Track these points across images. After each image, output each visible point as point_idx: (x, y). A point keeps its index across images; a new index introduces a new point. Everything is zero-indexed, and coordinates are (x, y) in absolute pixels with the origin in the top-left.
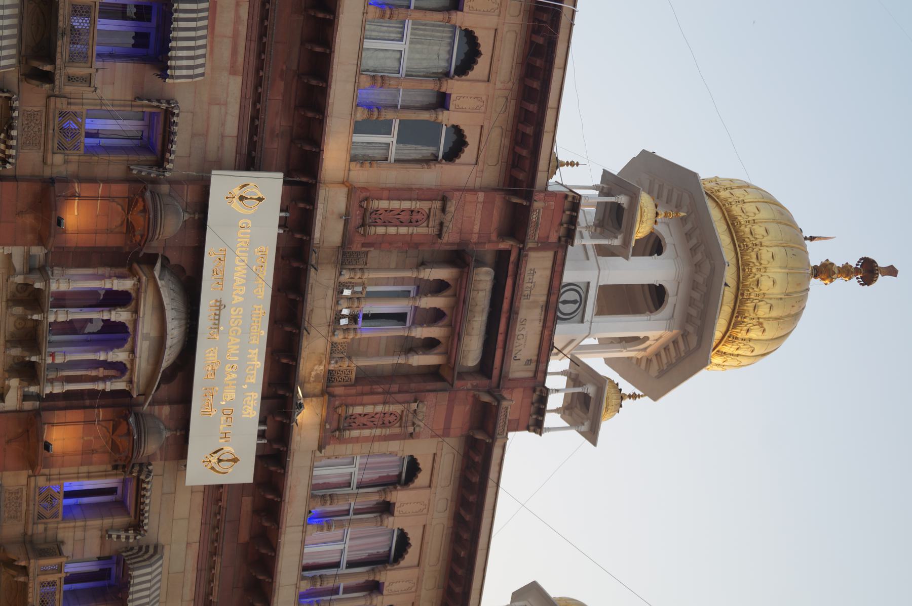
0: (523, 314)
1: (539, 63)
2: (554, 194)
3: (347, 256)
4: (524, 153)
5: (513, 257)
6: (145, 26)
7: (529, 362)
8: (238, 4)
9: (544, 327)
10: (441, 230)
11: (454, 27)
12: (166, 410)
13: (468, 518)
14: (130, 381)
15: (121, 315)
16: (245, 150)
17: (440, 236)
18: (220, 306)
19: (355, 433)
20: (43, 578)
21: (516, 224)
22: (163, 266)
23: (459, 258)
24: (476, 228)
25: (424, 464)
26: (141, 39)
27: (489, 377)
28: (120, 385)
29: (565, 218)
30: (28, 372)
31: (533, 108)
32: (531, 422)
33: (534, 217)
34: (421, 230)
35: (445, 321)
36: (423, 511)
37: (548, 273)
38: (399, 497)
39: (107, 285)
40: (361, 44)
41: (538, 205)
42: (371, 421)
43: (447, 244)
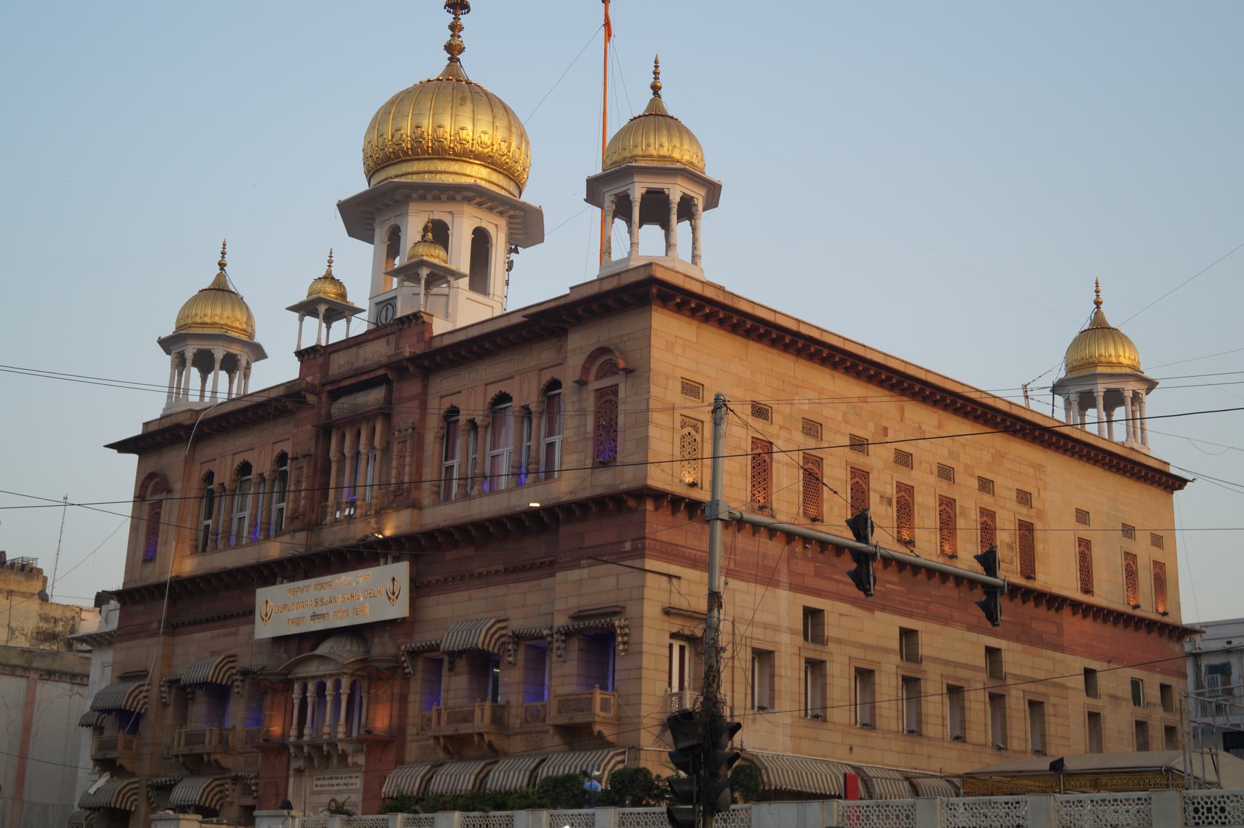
5: (329, 388)
9: (368, 341)
15: (311, 687)
18: (315, 616)
43: (316, 446)
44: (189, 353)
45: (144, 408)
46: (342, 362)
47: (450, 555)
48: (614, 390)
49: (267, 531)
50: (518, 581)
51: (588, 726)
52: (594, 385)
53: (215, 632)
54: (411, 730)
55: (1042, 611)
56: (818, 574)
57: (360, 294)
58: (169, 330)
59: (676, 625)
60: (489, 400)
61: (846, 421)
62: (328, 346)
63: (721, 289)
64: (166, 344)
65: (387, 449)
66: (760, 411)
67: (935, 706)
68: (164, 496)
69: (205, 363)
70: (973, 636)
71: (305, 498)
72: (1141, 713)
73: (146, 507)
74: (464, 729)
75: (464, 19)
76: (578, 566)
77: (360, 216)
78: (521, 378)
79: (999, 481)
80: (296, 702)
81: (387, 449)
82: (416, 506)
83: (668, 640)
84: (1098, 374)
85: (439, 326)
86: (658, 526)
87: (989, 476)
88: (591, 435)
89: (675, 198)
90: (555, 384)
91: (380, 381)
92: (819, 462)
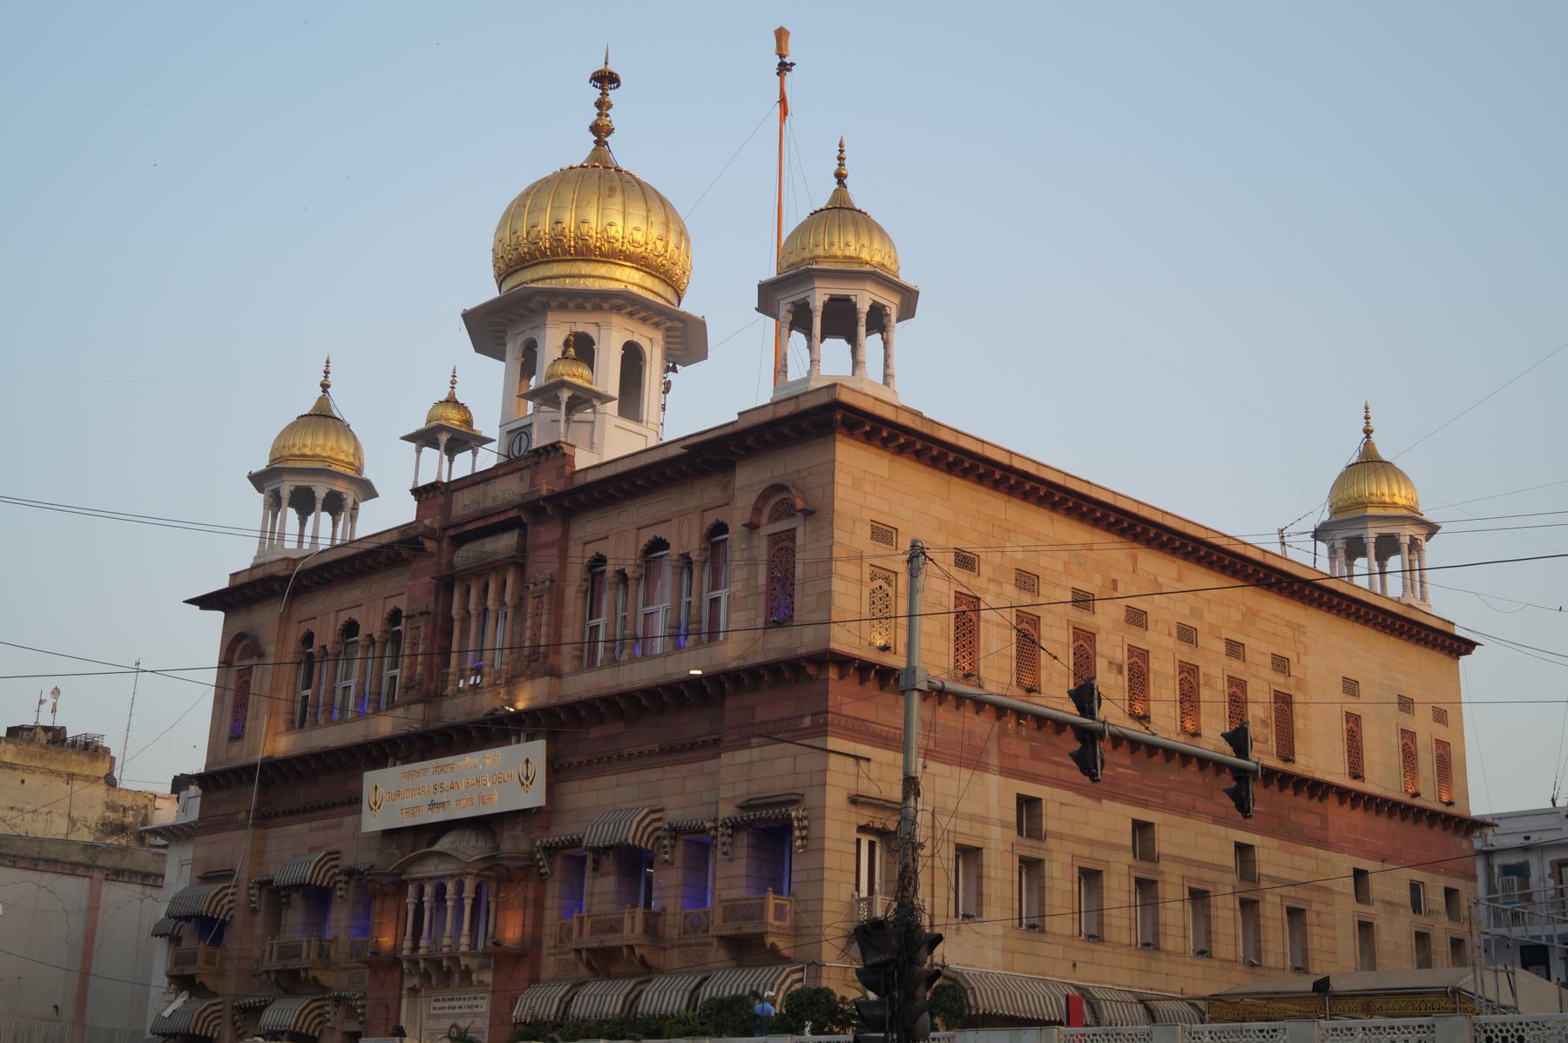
5: (452, 532)
15: (429, 890)
17: (427, 613)
18: (433, 805)
43: (436, 601)
44: (286, 490)
45: (235, 556)
46: (467, 502)
47: (595, 732)
48: (791, 535)
49: (377, 702)
50: (675, 763)
51: (760, 937)
52: (767, 529)
53: (315, 824)
54: (548, 942)
55: (1303, 800)
56: (1035, 756)
57: (488, 421)
58: (261, 463)
59: (865, 816)
60: (641, 547)
61: (1068, 572)
62: (450, 483)
63: (918, 414)
64: (258, 480)
65: (519, 606)
66: (965, 561)
67: (1175, 913)
68: (254, 661)
69: (304, 503)
70: (1221, 830)
71: (423, 663)
72: (1422, 922)
73: (233, 674)
74: (612, 940)
75: (613, 95)
77: (490, 328)
78: (680, 520)
79: (1251, 644)
80: (411, 908)
81: (519, 606)
82: (554, 673)
83: (855, 835)
84: (1367, 516)
85: (583, 459)
86: (843, 696)
87: (1238, 638)
88: (763, 589)
89: (864, 306)
90: (720, 528)
91: (512, 527)
92: (1035, 621)
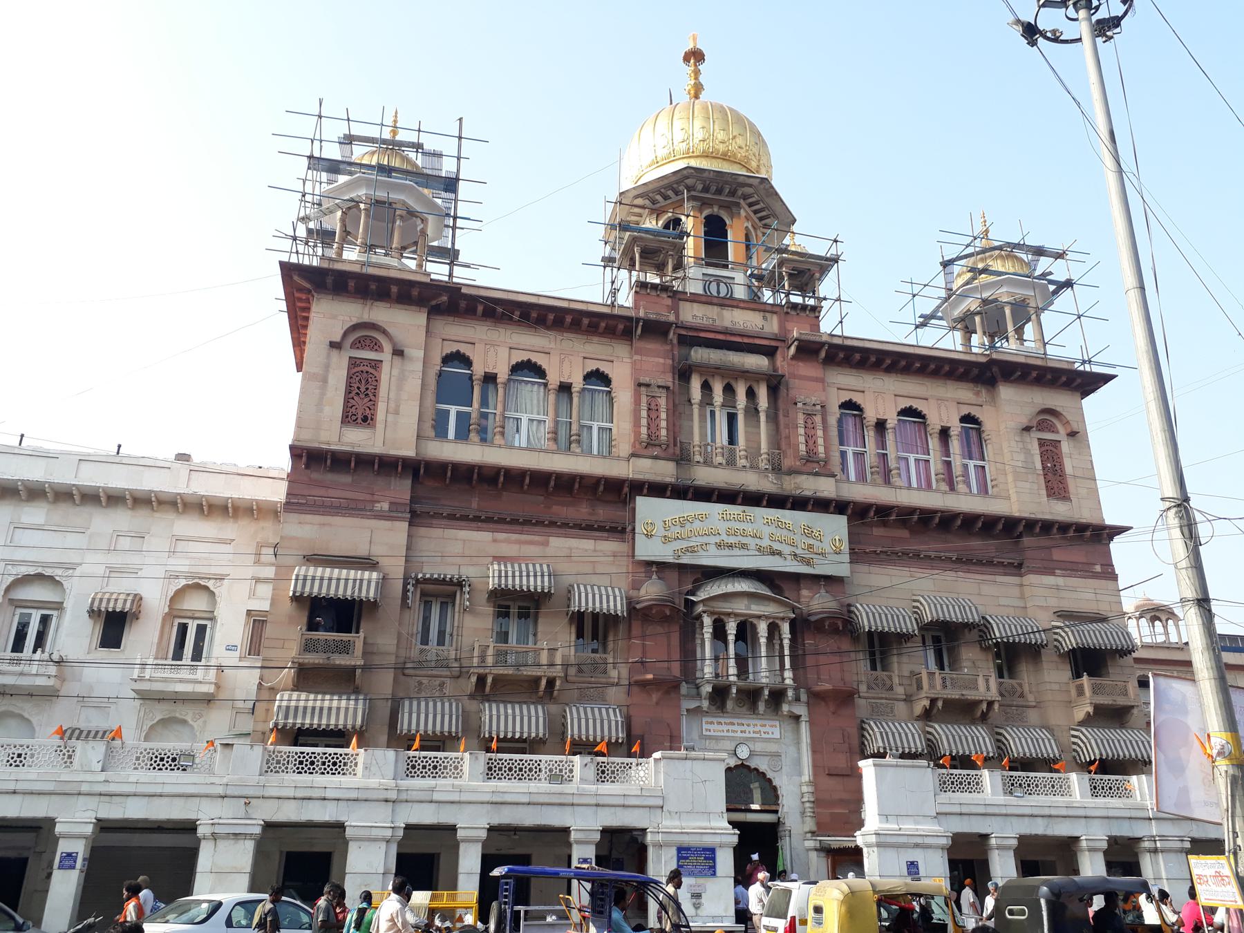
0: (727, 324)
1: (534, 315)
2: (636, 301)
3: (682, 458)
4: (603, 325)
5: (684, 333)
6: (514, 611)
7: (765, 318)
8: (495, 541)
9: (737, 307)
10: (663, 387)
11: (509, 380)
12: (805, 592)
13: (888, 361)
14: (783, 619)
15: (731, 628)
16: (605, 534)
17: (667, 388)
19: (821, 449)
20: (939, 687)
21: (655, 330)
22: (693, 595)
23: (684, 374)
24: (661, 361)
25: (845, 397)
26: (524, 615)
27: (777, 348)
28: (785, 628)
29: (654, 293)
30: (777, 696)
31: (569, 319)
32: (812, 315)
33: (652, 317)
34: (662, 402)
35: (734, 385)
36: (882, 397)
37: (695, 305)
38: (871, 415)
39: (707, 636)
40: (520, 448)
41: (642, 314)
42: (810, 438)
76: (1053, 574)
